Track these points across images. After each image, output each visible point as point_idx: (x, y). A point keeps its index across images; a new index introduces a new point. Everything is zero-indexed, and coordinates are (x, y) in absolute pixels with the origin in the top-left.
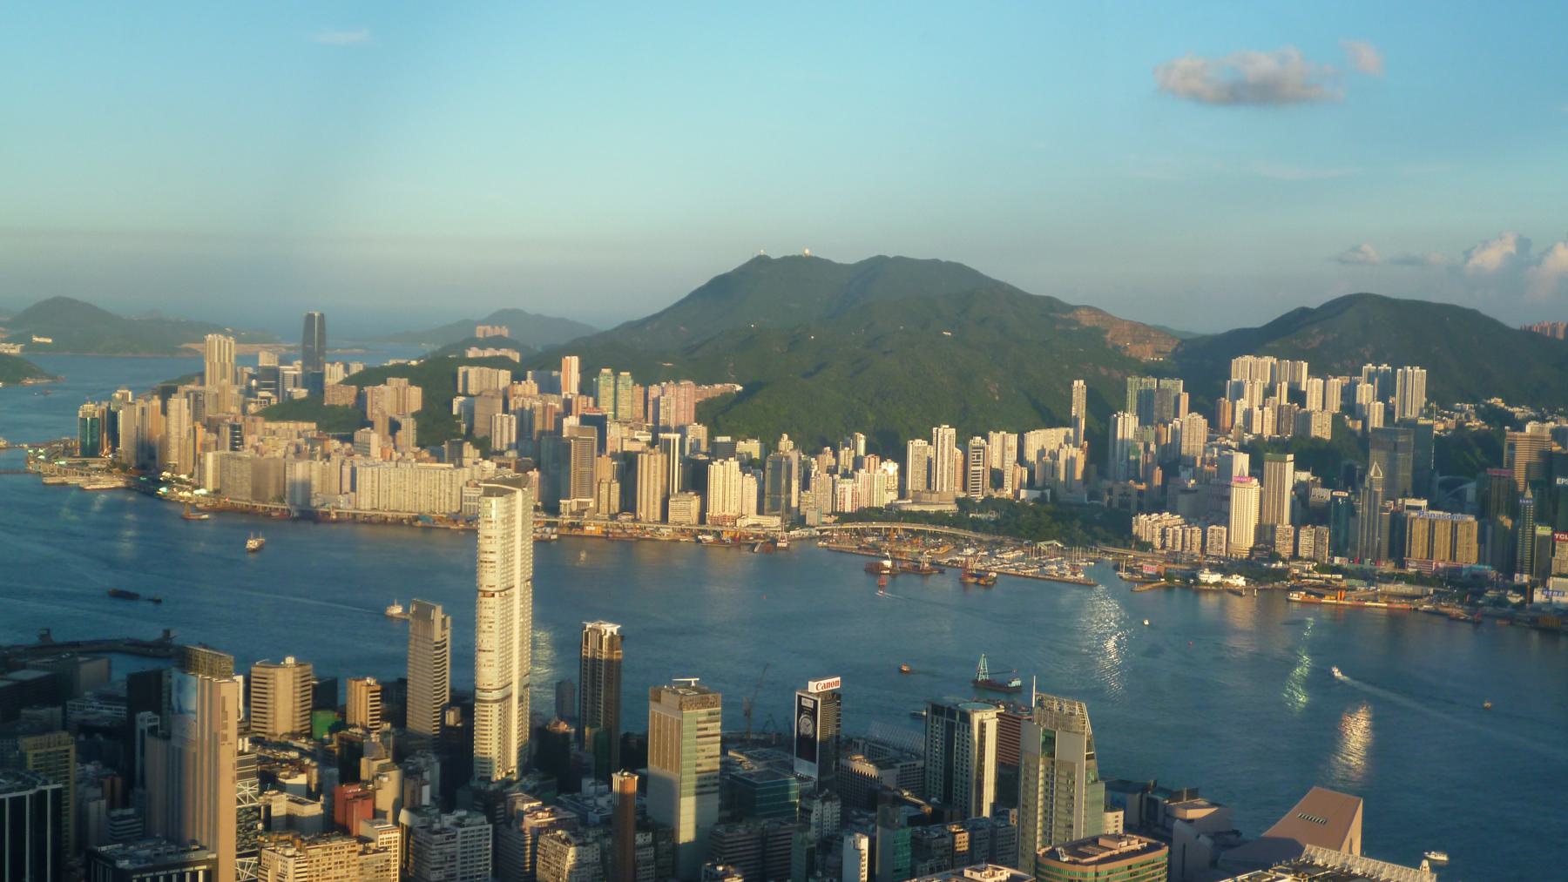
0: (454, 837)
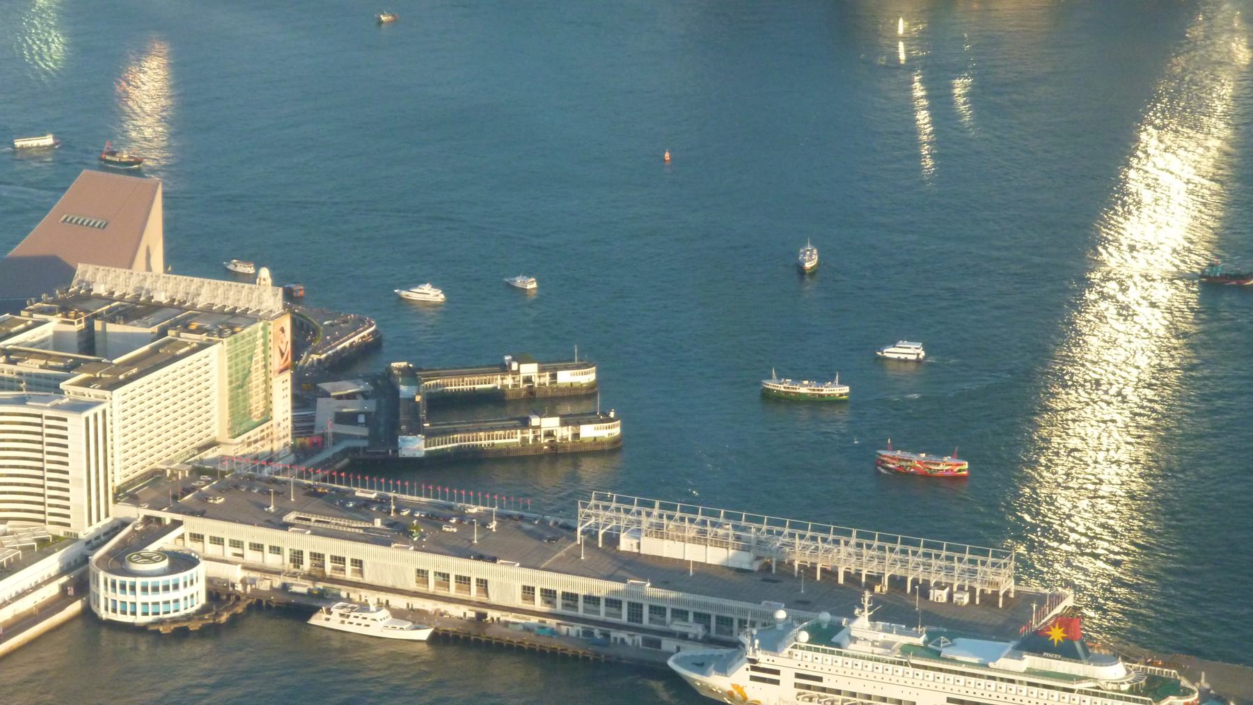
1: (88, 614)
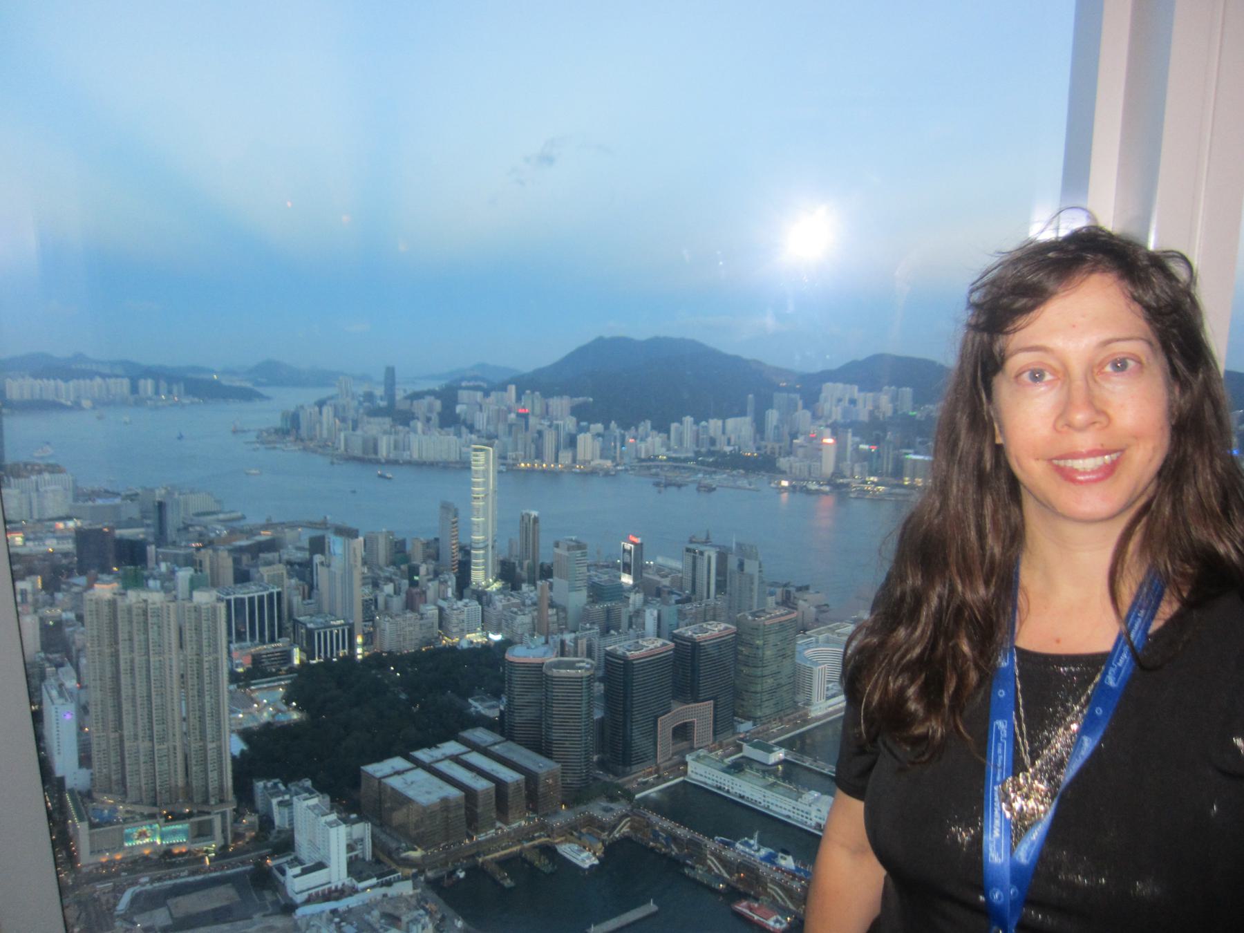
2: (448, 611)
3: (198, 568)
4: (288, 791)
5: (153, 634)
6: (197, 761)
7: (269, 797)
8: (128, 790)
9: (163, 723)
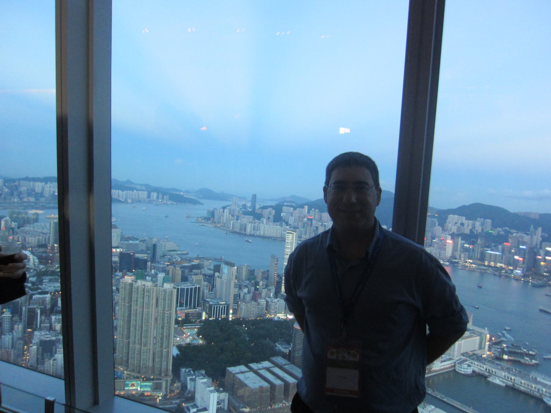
0: (277, 304)
1: (455, 370)
2: (270, 303)
3: (167, 274)
4: (195, 374)
5: (146, 300)
6: (158, 356)
7: (186, 376)
8: (129, 365)
9: (146, 338)
